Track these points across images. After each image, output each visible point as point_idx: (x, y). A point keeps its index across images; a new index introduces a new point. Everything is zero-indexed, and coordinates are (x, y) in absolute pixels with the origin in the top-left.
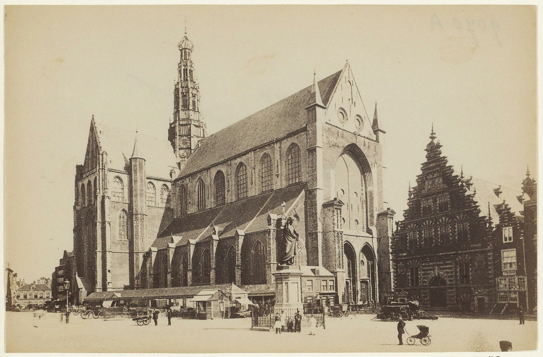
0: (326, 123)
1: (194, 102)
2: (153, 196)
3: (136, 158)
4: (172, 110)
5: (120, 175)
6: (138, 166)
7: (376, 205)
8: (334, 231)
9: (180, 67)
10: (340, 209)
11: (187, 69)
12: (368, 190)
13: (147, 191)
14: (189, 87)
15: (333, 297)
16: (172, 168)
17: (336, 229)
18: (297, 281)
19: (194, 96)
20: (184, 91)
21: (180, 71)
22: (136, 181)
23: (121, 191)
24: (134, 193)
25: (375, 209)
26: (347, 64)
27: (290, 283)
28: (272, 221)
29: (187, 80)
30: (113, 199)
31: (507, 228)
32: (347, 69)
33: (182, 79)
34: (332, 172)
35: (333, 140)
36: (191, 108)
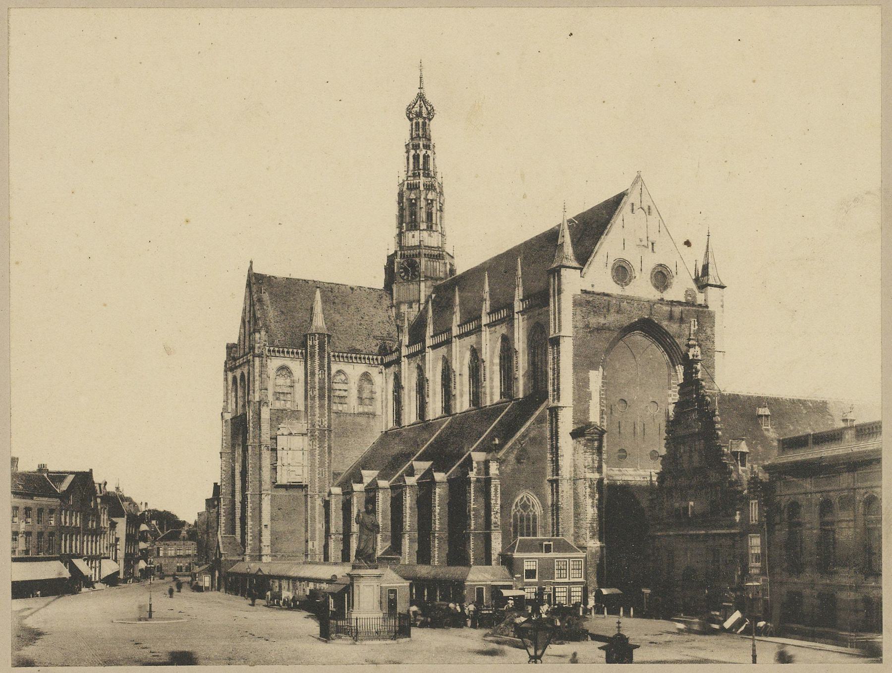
0: (584, 292)
1: (429, 215)
2: (344, 394)
3: (314, 334)
8: (585, 479)
9: (408, 152)
11: (418, 155)
13: (336, 386)
14: (422, 188)
19: (430, 203)
20: (413, 196)
21: (408, 160)
24: (310, 393)
26: (639, 177)
28: (475, 465)
30: (279, 405)
31: (754, 502)
32: (638, 187)
33: (410, 173)
35: (594, 321)
36: (423, 226)
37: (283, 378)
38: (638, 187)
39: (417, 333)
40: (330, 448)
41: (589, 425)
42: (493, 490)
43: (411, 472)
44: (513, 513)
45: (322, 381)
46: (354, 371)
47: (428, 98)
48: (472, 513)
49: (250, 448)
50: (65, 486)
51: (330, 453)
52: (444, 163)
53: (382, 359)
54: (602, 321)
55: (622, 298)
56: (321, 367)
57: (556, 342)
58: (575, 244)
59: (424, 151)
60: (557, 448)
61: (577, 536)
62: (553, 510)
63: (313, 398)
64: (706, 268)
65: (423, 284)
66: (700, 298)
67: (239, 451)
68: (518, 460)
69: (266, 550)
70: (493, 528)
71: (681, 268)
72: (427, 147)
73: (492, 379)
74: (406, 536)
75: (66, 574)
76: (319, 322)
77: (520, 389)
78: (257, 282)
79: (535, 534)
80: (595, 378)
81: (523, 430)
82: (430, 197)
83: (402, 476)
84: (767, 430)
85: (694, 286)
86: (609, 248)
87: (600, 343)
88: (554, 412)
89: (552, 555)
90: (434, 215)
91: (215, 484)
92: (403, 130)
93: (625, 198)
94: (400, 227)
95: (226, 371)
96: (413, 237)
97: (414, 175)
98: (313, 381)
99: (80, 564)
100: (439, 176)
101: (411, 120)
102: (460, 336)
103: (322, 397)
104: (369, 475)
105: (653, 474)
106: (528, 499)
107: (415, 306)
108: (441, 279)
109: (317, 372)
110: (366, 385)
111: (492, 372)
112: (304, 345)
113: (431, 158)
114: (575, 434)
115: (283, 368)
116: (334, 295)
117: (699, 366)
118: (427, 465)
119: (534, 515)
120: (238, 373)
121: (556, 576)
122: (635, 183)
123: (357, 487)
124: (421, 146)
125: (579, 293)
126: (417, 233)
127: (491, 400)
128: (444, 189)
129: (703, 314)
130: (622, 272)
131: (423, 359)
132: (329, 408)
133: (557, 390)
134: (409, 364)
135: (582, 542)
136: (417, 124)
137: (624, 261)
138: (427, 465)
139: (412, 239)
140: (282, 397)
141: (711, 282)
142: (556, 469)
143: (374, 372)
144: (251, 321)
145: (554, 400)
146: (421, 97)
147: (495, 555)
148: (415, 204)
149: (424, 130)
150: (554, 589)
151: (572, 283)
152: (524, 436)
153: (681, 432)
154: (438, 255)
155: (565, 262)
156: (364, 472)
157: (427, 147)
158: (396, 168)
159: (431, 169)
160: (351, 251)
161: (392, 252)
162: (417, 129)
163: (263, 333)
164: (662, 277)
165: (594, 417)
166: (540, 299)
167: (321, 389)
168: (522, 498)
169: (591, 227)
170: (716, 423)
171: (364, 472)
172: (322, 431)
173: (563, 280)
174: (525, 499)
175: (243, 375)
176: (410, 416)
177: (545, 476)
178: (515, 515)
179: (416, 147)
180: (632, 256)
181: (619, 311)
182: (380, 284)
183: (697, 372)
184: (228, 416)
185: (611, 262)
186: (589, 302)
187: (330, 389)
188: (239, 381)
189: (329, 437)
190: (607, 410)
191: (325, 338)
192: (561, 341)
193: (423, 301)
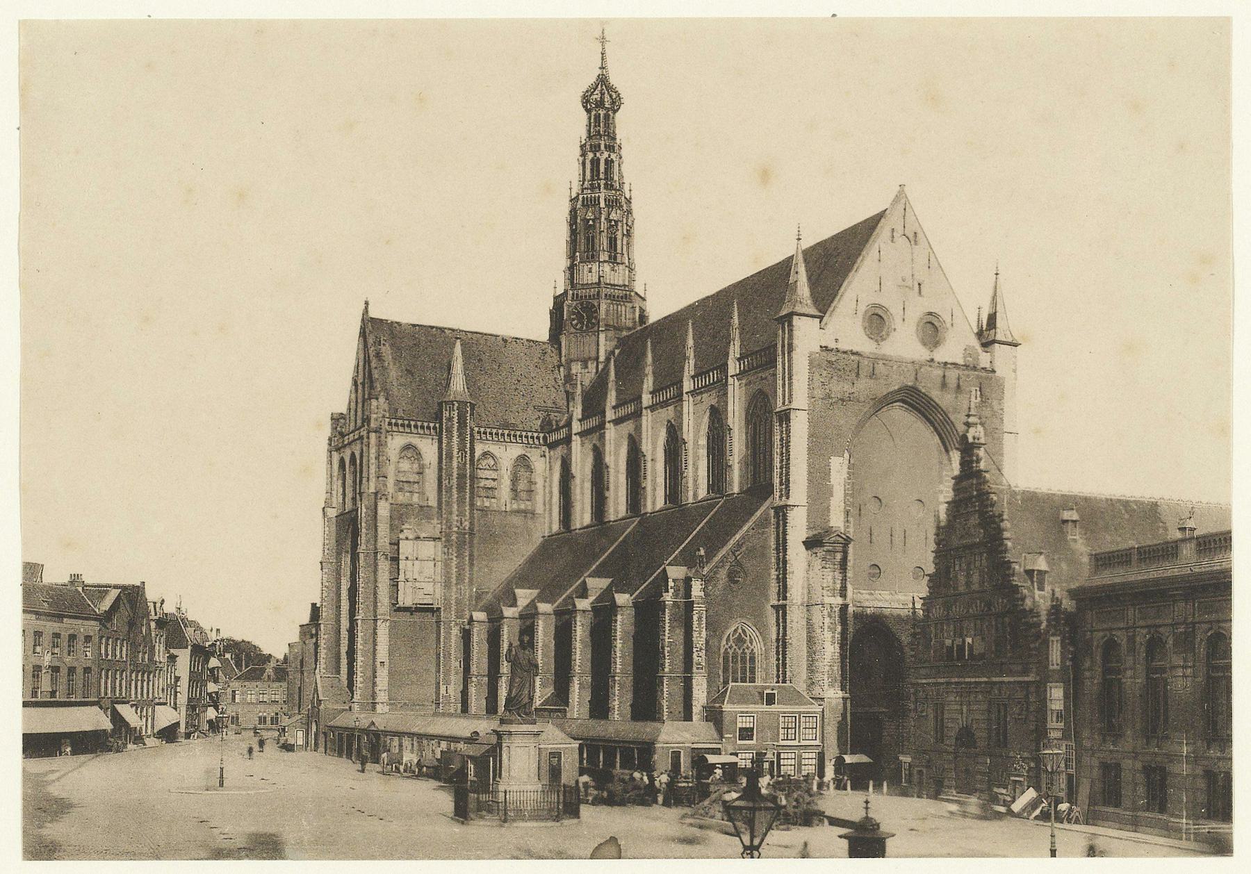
0: (825, 348)
1: (613, 242)
4: (564, 263)
6: (456, 420)
9: (584, 155)
11: (599, 160)
13: (481, 474)
14: (602, 205)
16: (542, 415)
19: (612, 225)
20: (590, 215)
21: (584, 164)
22: (450, 456)
23: (416, 478)
24: (445, 482)
28: (671, 584)
30: (402, 498)
31: (1054, 639)
35: (840, 388)
36: (604, 256)
37: (409, 459)
38: (900, 207)
39: (593, 404)
40: (471, 555)
41: (828, 531)
42: (695, 618)
43: (583, 592)
44: (722, 651)
45: (462, 468)
46: (507, 454)
47: (614, 80)
48: (667, 649)
49: (361, 556)
50: (106, 605)
51: (472, 565)
52: (635, 171)
53: (545, 438)
54: (847, 387)
55: (875, 359)
56: (462, 449)
57: (785, 417)
58: (814, 282)
59: (606, 154)
60: (785, 562)
61: (811, 684)
62: (778, 647)
63: (449, 489)
64: (992, 319)
65: (602, 336)
66: (984, 359)
67: (346, 560)
68: (732, 577)
69: (382, 697)
70: (695, 670)
71: (958, 320)
72: (610, 148)
73: (696, 469)
75: (106, 724)
76: (458, 383)
77: (735, 482)
78: (374, 330)
79: (753, 680)
80: (838, 468)
81: (738, 536)
82: (613, 216)
83: (570, 597)
84: (1075, 541)
85: (975, 343)
86: (858, 290)
87: (845, 419)
88: (781, 513)
89: (774, 708)
90: (619, 242)
91: (314, 605)
92: (577, 124)
94: (572, 257)
97: (592, 188)
98: (451, 467)
99: (126, 712)
100: (626, 188)
101: (588, 111)
102: (652, 408)
103: (461, 488)
104: (524, 596)
105: (917, 599)
106: (744, 631)
107: (592, 366)
108: (629, 329)
109: (455, 453)
110: (523, 473)
111: (696, 457)
112: (438, 417)
113: (616, 164)
114: (810, 544)
115: (408, 447)
116: (483, 351)
117: (981, 452)
118: (604, 583)
119: (752, 652)
120: (347, 455)
121: (781, 737)
122: (897, 199)
123: (509, 612)
124: (602, 147)
125: (818, 349)
126: (595, 267)
127: (695, 495)
128: (634, 206)
129: (988, 384)
130: (877, 321)
131: (602, 437)
132: (472, 505)
133: (786, 483)
134: (583, 444)
135: (817, 691)
136: (597, 117)
137: (881, 307)
138: (604, 583)
139: (589, 274)
140: (406, 487)
141: (999, 337)
142: (783, 592)
143: (535, 456)
144: (366, 382)
145: (781, 497)
146: (603, 80)
147: (697, 709)
148: (594, 226)
149: (607, 126)
150: (779, 754)
151: (808, 336)
152: (739, 545)
153: (955, 542)
154: (625, 295)
155: (798, 309)
156: (519, 592)
158: (567, 174)
159: (616, 178)
160: (507, 290)
161: (560, 291)
163: (382, 400)
164: (932, 330)
165: (837, 520)
166: (765, 358)
167: (461, 477)
168: (735, 631)
169: (834, 260)
170: (1004, 530)
171: (519, 592)
172: (461, 534)
173: (797, 333)
175: (353, 454)
176: (583, 516)
177: (768, 600)
178: (726, 652)
180: (891, 300)
181: (873, 375)
182: (545, 336)
183: (978, 461)
184: (332, 513)
185: (862, 308)
186: (833, 361)
187: (473, 478)
189: (471, 542)
190: (854, 510)
192: (792, 416)
193: (602, 359)
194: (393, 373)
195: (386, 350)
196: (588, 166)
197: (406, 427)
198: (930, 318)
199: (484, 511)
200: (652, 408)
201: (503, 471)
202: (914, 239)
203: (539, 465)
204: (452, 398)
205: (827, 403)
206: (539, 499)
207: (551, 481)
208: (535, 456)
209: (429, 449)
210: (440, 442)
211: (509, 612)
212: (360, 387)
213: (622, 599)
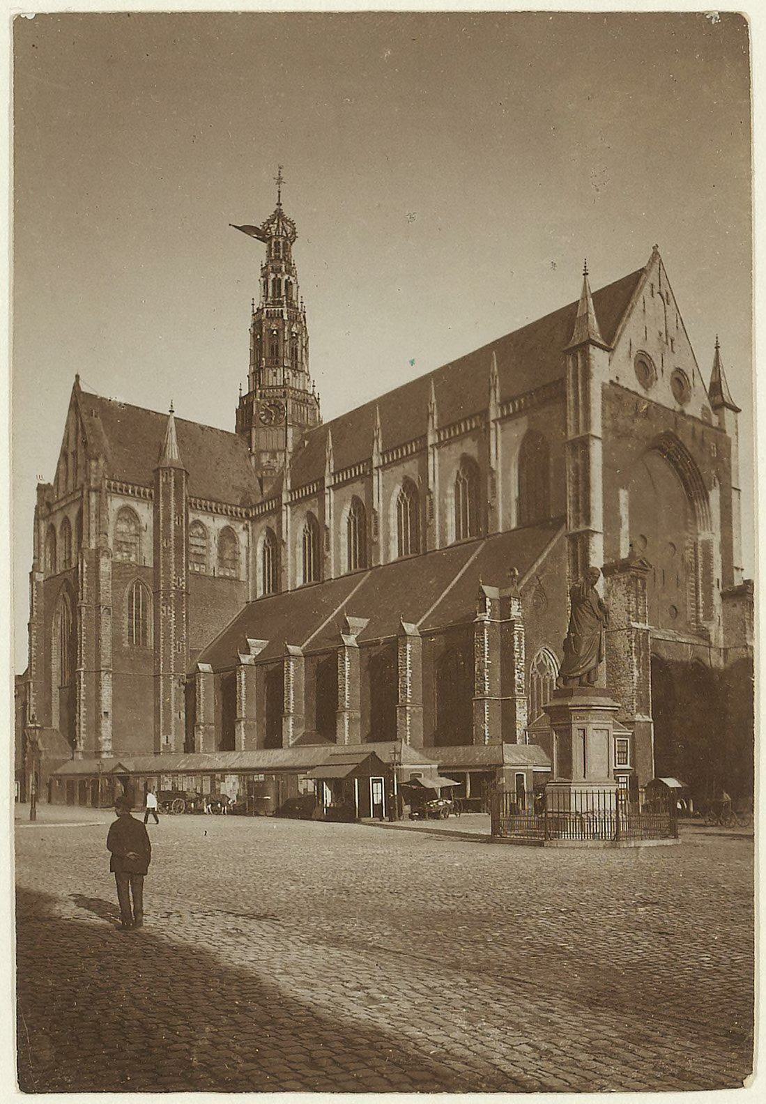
0: (611, 382)
1: (294, 352)
5: (134, 504)
7: (717, 574)
8: (630, 629)
9: (265, 276)
10: (643, 579)
11: (280, 280)
12: (700, 538)
13: (192, 541)
14: (285, 318)
15: (624, 780)
17: (634, 624)
18: (606, 727)
19: (294, 338)
20: (274, 326)
21: (266, 283)
22: (167, 519)
24: (163, 544)
25: (715, 583)
27: (590, 728)
28: (488, 603)
29: (280, 303)
32: (656, 266)
34: (623, 495)
37: (125, 527)
42: (516, 638)
46: (216, 524)
49: (83, 610)
53: (247, 514)
59: (286, 277)
63: (167, 551)
72: (289, 272)
73: (443, 516)
74: (346, 715)
78: (81, 403)
86: (637, 330)
90: (299, 352)
93: (644, 276)
95: (37, 519)
96: (275, 374)
102: (384, 467)
103: (178, 549)
109: (172, 516)
111: (443, 507)
112: (155, 484)
113: (295, 287)
115: (126, 509)
120: (58, 521)
123: (245, 659)
124: (283, 270)
126: (279, 371)
127: (443, 542)
130: (644, 366)
134: (293, 514)
139: (275, 377)
143: (239, 528)
146: (279, 214)
154: (309, 401)
157: (289, 272)
161: (245, 392)
162: (277, 251)
163: (101, 462)
164: (680, 382)
169: (616, 301)
174: (542, 657)
175: (66, 521)
179: (277, 271)
180: (652, 349)
184: (40, 577)
188: (58, 530)
191: (182, 474)
194: (106, 442)
195: (98, 421)
196: (270, 284)
197: (122, 493)
198: (678, 375)
199: (195, 574)
200: (384, 467)
201: (212, 540)
202: (666, 299)
203: (243, 538)
204: (168, 464)
205: (615, 433)
206: (243, 567)
207: (255, 551)
208: (239, 528)
209: (145, 513)
210: (156, 508)
211: (245, 659)
212: (70, 456)
213: (410, 628)
